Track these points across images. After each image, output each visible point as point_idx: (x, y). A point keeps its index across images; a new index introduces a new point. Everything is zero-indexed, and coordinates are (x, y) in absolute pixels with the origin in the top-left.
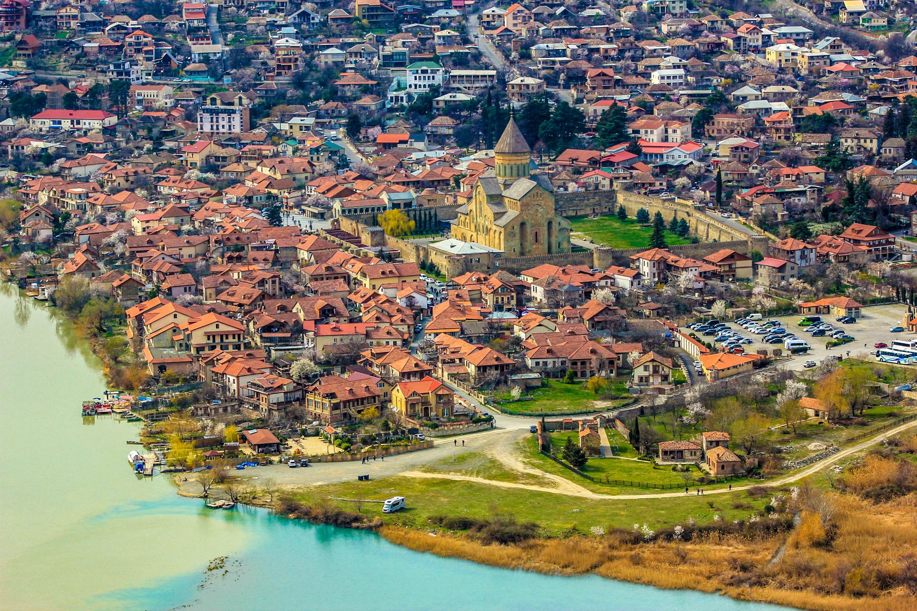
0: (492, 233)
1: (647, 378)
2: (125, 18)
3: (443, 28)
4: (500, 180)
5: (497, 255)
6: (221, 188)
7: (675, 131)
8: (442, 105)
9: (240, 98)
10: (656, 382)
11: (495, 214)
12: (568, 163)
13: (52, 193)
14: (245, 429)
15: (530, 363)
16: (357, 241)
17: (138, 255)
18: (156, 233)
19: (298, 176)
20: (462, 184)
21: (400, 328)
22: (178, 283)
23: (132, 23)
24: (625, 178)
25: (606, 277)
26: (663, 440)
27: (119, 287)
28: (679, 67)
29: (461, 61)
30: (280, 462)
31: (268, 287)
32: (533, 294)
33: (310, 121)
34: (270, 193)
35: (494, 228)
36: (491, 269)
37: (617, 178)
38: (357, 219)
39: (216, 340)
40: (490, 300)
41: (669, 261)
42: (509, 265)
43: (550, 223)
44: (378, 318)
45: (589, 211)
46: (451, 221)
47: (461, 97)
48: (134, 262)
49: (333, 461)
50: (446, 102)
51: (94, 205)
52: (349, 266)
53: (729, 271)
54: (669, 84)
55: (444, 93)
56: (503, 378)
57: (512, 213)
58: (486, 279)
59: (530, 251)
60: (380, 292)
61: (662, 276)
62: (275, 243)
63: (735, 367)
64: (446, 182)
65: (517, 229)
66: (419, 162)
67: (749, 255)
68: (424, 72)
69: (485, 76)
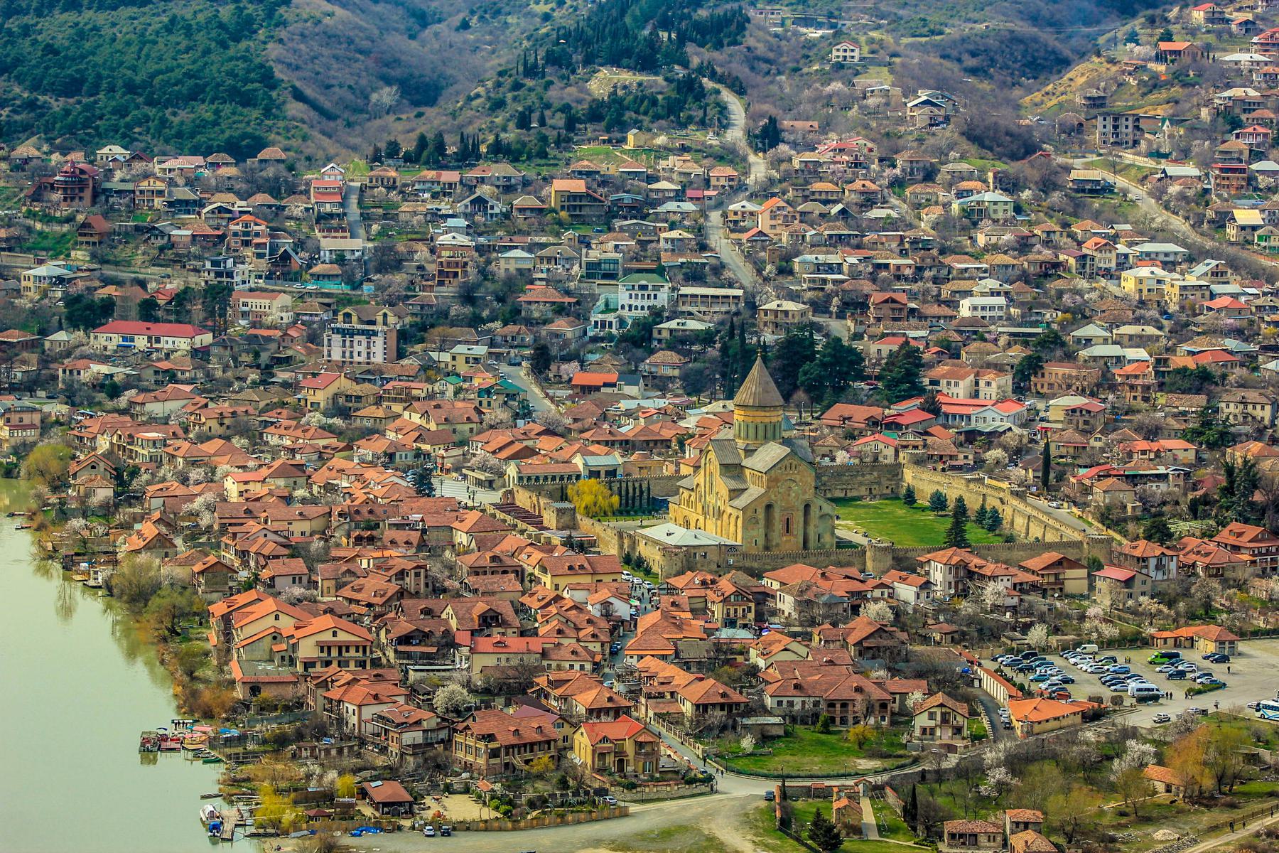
0: (725, 517)
1: (933, 730)
2: (231, 197)
3: (671, 229)
4: (741, 443)
5: (732, 548)
6: (352, 440)
7: (988, 384)
8: (666, 335)
9: (385, 315)
10: (945, 736)
11: (731, 491)
12: (837, 423)
13: (115, 438)
14: (365, 780)
15: (769, 702)
16: (537, 522)
17: (231, 529)
18: (258, 499)
19: (459, 427)
20: (687, 448)
21: (591, 646)
22: (284, 570)
23: (240, 205)
24: (915, 447)
25: (882, 586)
26: (951, 817)
27: (202, 572)
28: (999, 294)
29: (695, 275)
30: (413, 828)
31: (410, 581)
32: (779, 605)
33: (481, 350)
34: (420, 449)
35: (729, 510)
36: (722, 568)
37: (906, 447)
38: (539, 491)
39: (332, 653)
40: (718, 611)
41: (972, 567)
42: (748, 564)
43: (807, 507)
44: (560, 632)
45: (863, 491)
46: (670, 499)
47: (693, 325)
48: (224, 539)
49: (486, 830)
50: (671, 331)
51: (173, 456)
52: (524, 556)
53: (1055, 584)
54: (983, 318)
55: (669, 319)
56: (730, 722)
57: (755, 490)
58: (713, 582)
59: (777, 545)
60: (565, 595)
61: (960, 587)
62: (422, 520)
63: (1055, 719)
64: (666, 443)
65: (761, 515)
66: (629, 414)
67: (1084, 562)
68: (644, 288)
69: (728, 297)
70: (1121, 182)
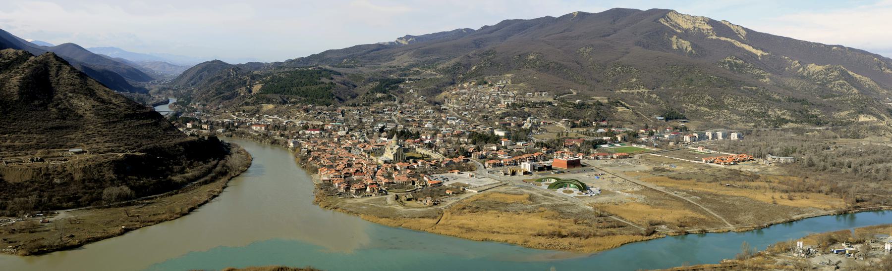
16: (365, 156)
38: (366, 153)
57: (395, 151)
70: (448, 108)
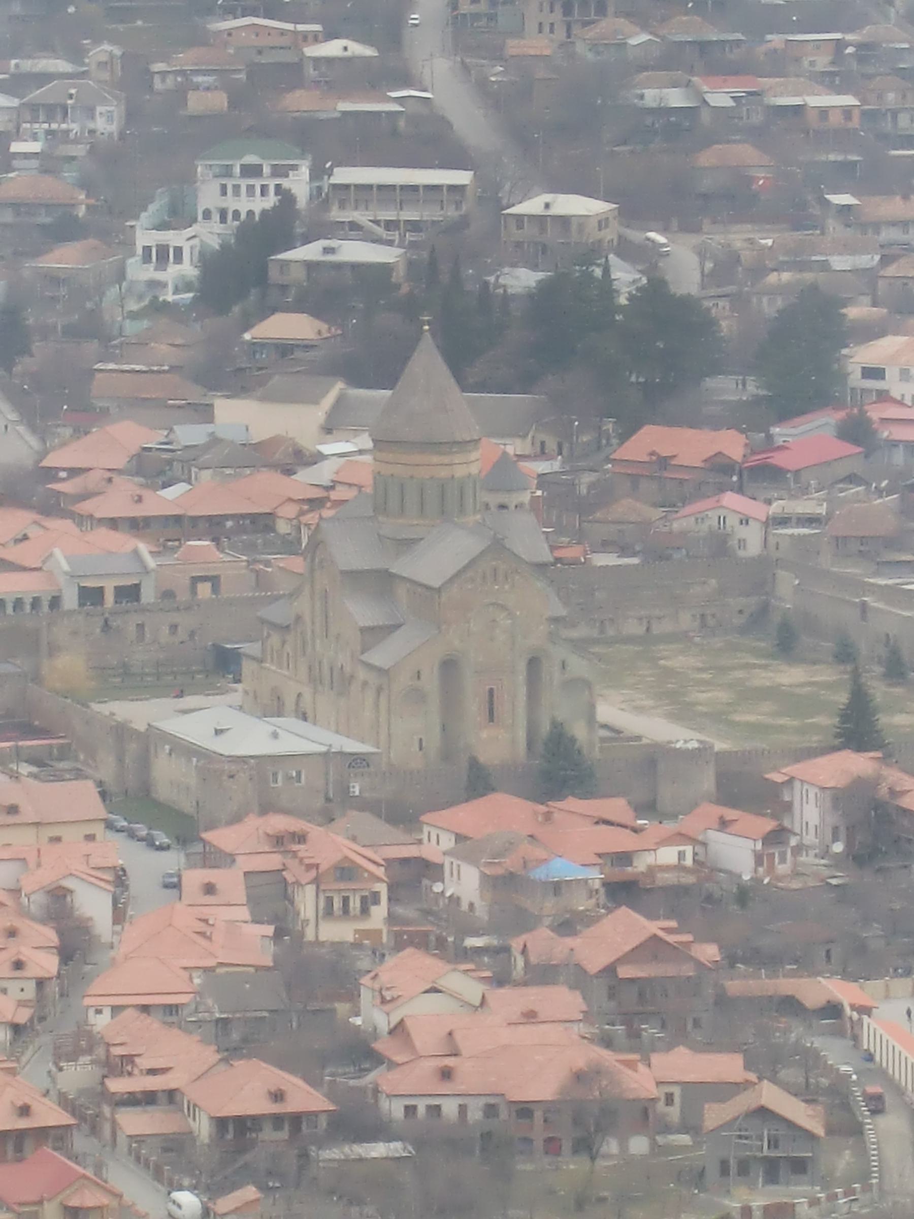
5: (357, 761)
35: (362, 674)
43: (534, 664)
46: (246, 648)
50: (311, 266)
55: (307, 240)
65: (431, 683)
